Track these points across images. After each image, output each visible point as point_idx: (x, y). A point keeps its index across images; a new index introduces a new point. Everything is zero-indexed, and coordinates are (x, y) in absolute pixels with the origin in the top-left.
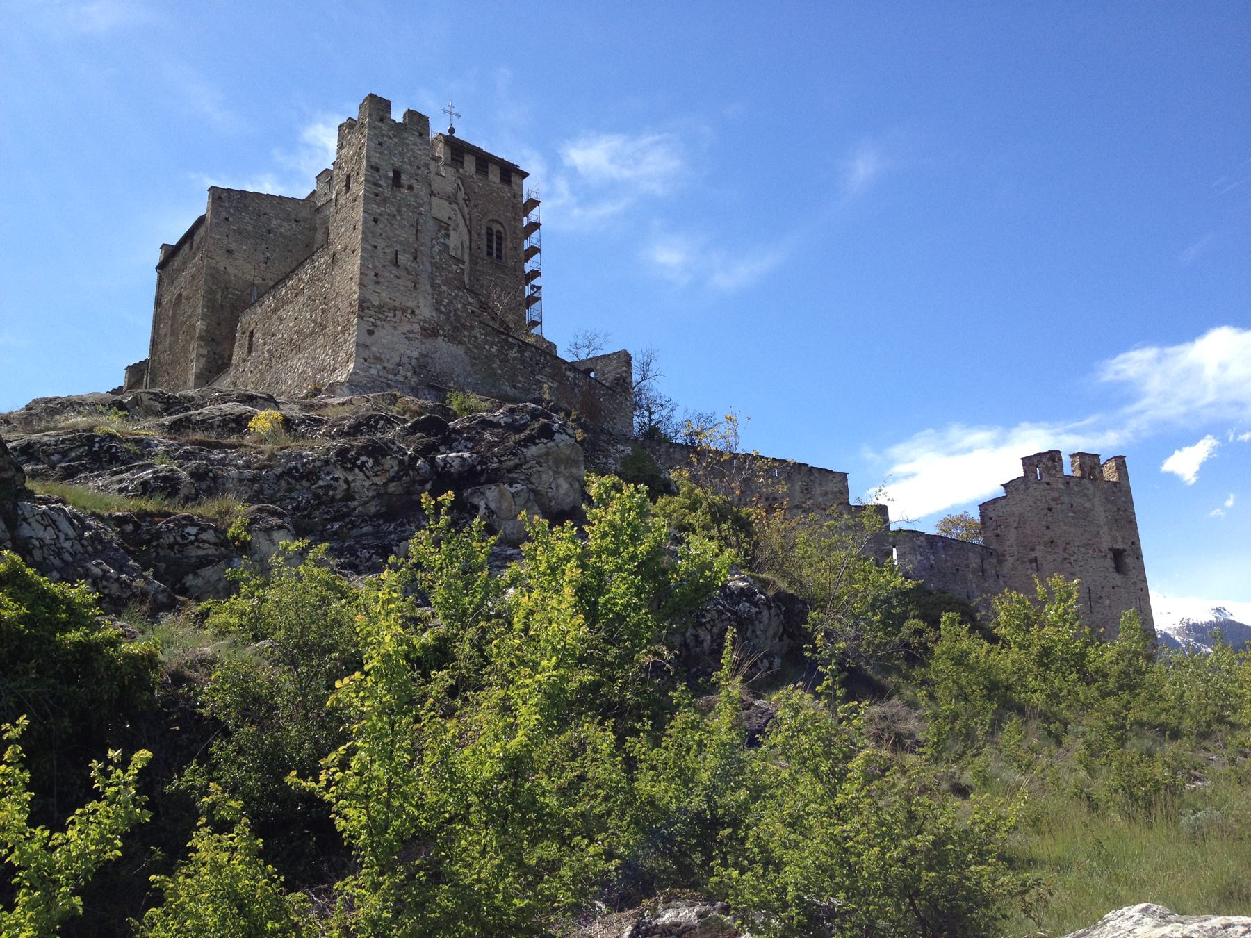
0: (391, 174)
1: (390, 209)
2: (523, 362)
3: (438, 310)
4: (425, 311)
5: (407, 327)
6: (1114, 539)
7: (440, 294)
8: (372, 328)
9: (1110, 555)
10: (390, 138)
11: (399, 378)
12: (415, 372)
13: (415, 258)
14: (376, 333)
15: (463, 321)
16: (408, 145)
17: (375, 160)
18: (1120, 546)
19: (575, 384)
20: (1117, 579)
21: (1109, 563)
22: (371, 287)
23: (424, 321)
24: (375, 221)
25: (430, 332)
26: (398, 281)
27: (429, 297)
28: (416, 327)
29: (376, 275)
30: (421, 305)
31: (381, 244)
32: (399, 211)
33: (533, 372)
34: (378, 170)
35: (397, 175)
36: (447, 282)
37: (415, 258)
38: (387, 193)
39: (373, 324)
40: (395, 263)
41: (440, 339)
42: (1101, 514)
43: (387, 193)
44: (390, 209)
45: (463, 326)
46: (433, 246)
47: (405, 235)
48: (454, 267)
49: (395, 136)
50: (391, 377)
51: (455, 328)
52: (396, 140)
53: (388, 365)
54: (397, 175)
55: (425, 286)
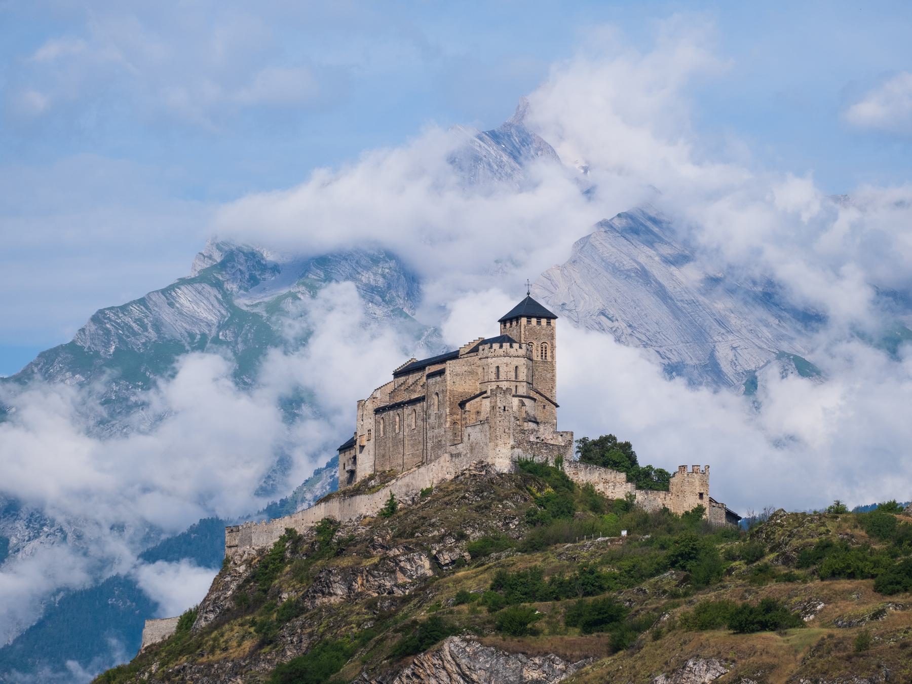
1: (503, 418)
2: (537, 448)
6: (701, 490)
18: (702, 492)
21: (698, 497)
35: (504, 407)
38: (502, 414)
42: (697, 483)
43: (502, 414)
44: (503, 418)
51: (519, 445)
54: (504, 407)
55: (512, 436)
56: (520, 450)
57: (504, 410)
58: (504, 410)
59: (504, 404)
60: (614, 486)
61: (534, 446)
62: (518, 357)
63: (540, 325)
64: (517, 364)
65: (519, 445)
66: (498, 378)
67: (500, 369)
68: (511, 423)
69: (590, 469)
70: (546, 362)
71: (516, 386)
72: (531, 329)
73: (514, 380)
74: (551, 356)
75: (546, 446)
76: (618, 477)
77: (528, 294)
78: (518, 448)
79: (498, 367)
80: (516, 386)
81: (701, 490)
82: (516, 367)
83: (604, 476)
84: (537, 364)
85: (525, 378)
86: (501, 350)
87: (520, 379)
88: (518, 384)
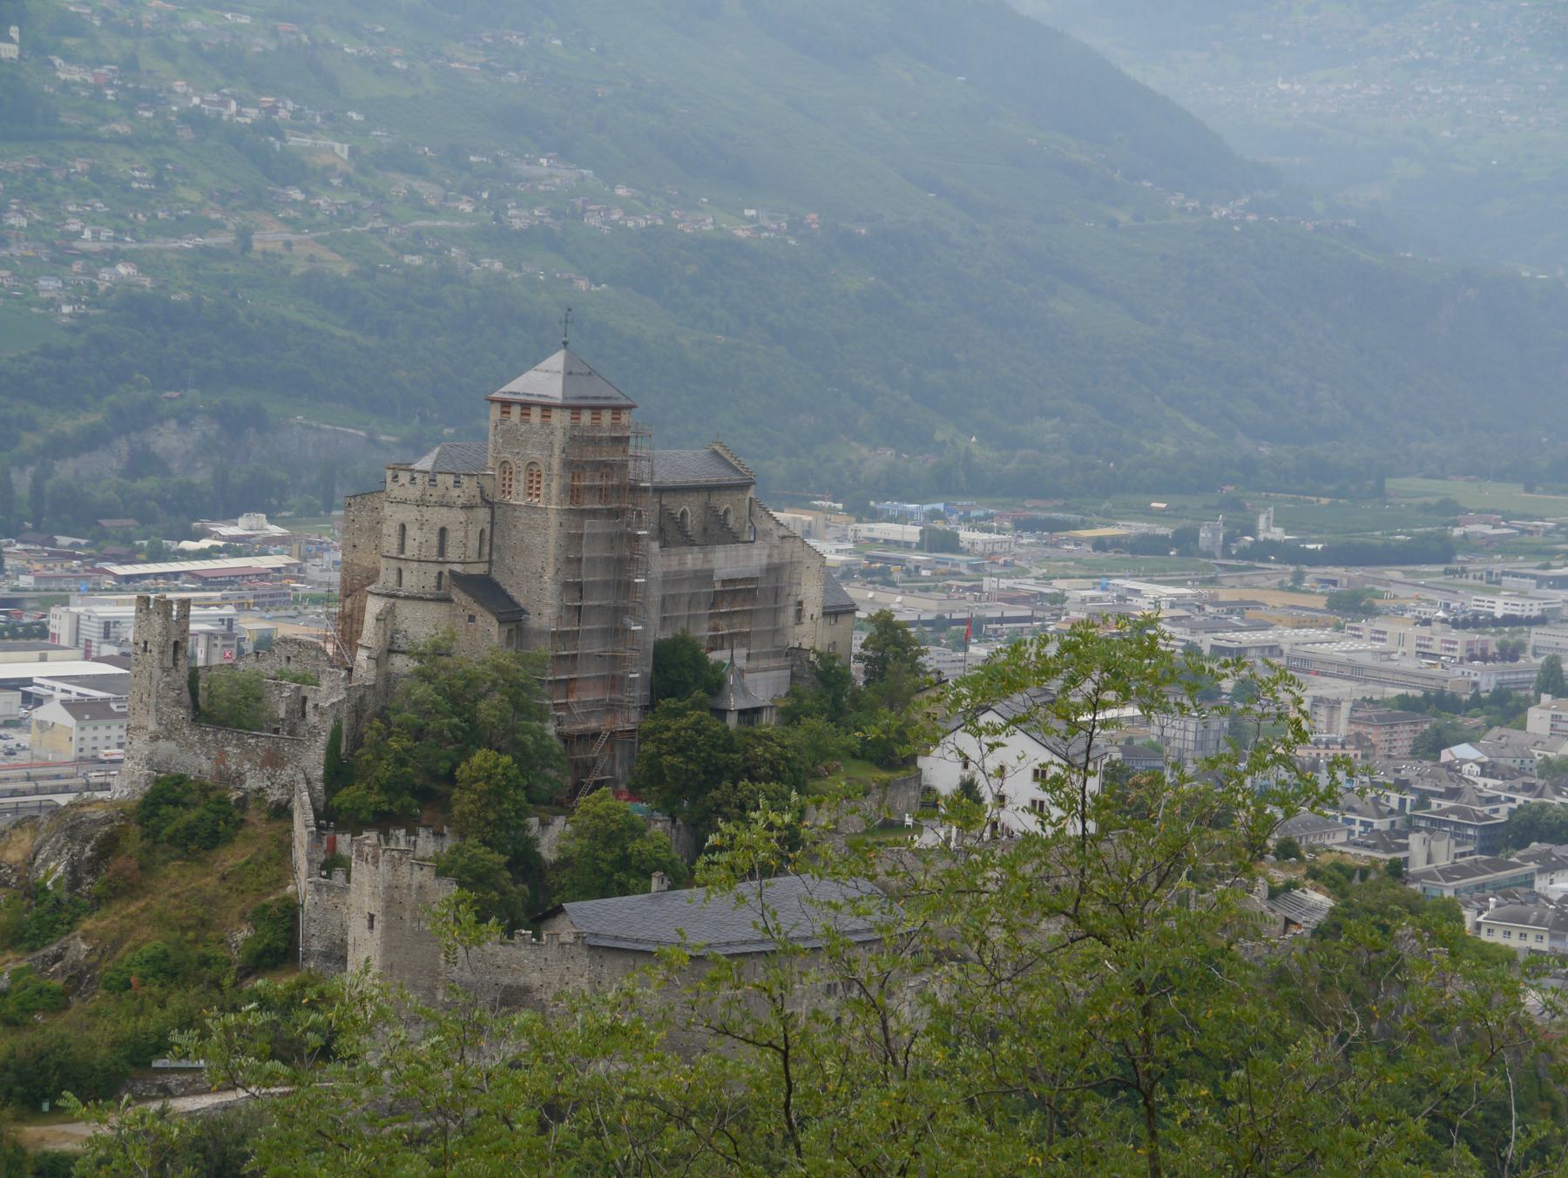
2: (216, 741)
3: (160, 724)
7: (163, 714)
25: (155, 738)
35: (146, 643)
43: (140, 657)
47: (146, 682)
54: (146, 643)
55: (153, 712)
56: (172, 745)
57: (145, 649)
58: (145, 649)
59: (145, 636)
61: (210, 737)
62: (405, 502)
63: (527, 422)
68: (154, 683)
71: (400, 571)
72: (508, 431)
75: (238, 740)
78: (168, 738)
80: (400, 571)
82: (403, 527)
84: (517, 514)
87: (408, 554)
88: (402, 565)
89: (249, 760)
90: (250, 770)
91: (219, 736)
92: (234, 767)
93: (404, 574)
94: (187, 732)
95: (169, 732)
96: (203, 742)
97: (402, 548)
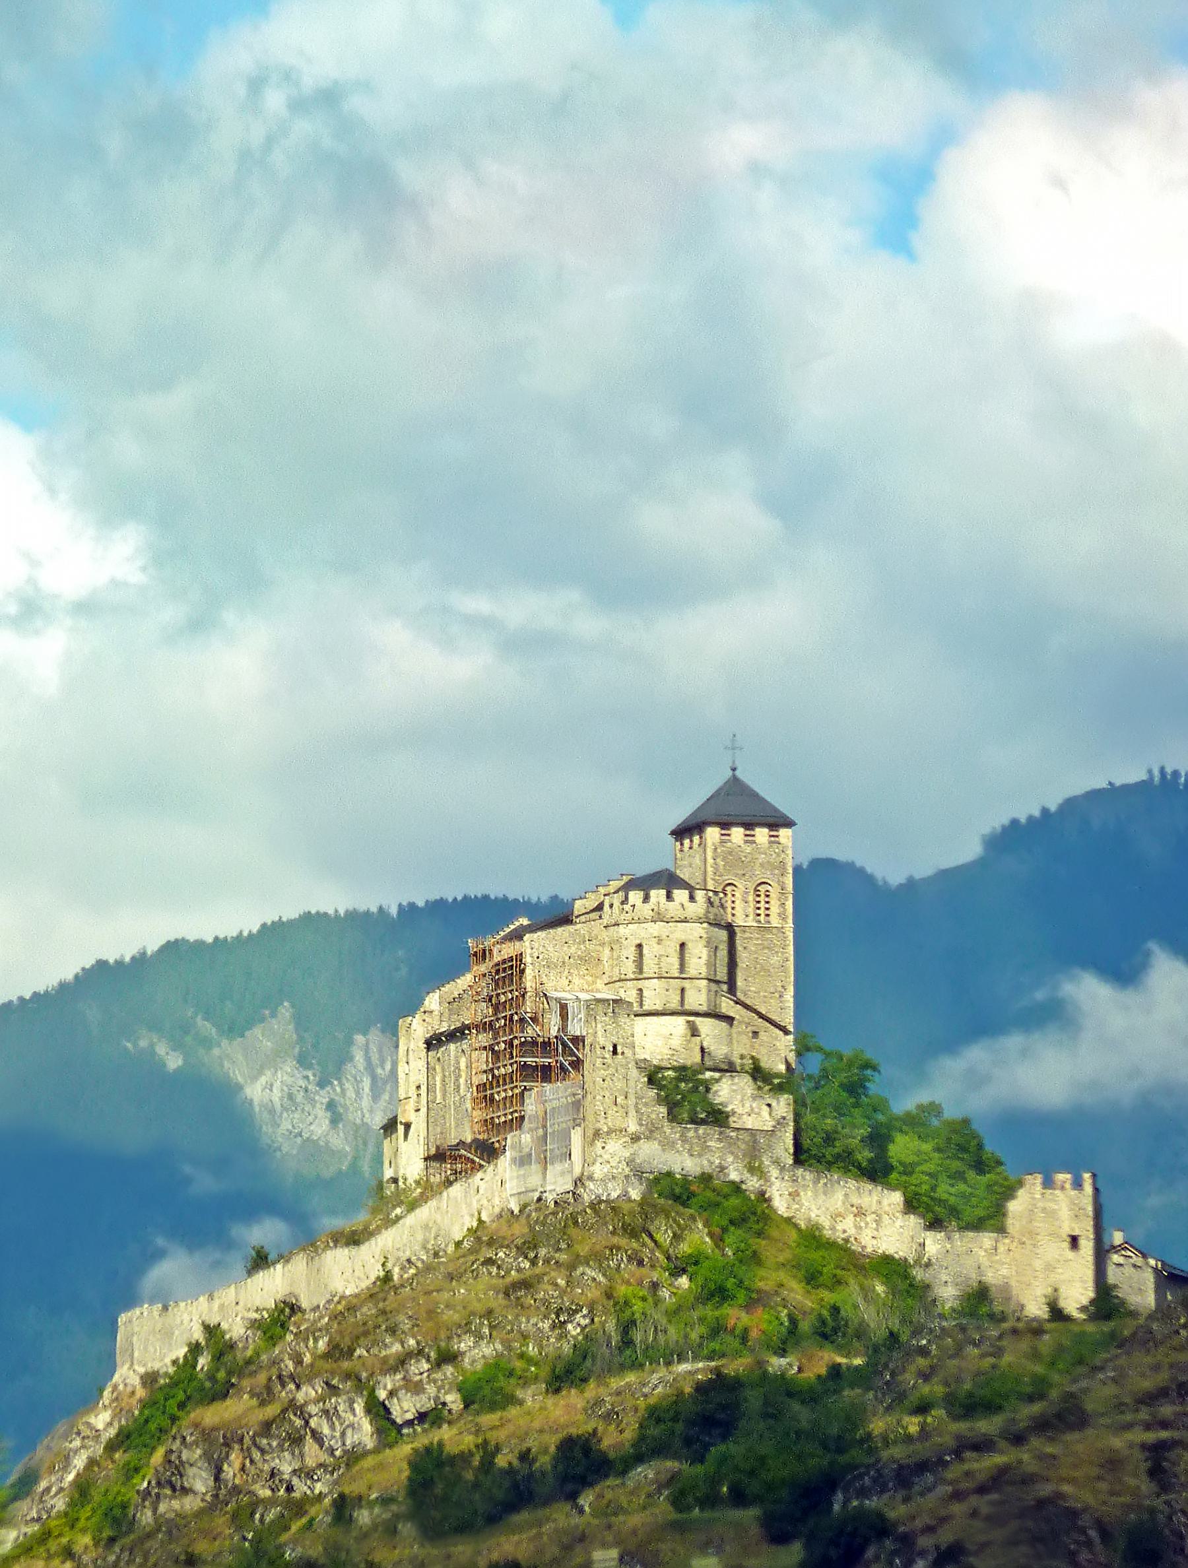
0: (611, 1049)
2: (698, 1137)
3: (641, 1125)
4: (633, 1127)
5: (624, 1140)
8: (604, 1145)
9: (1069, 1239)
10: (610, 1025)
11: (620, 1170)
12: (628, 1165)
13: (626, 1098)
14: (606, 1148)
15: (656, 1126)
16: (621, 1025)
17: (602, 1043)
19: (738, 1139)
20: (1070, 1254)
21: (1066, 1245)
22: (603, 1121)
23: (633, 1134)
24: (604, 1080)
25: (635, 1139)
26: (618, 1114)
27: (634, 1119)
28: (627, 1139)
29: (605, 1113)
30: (630, 1125)
31: (607, 1095)
32: (617, 1071)
33: (705, 1142)
34: (604, 1048)
35: (615, 1047)
36: (646, 1104)
37: (626, 1098)
38: (609, 1061)
39: (605, 1142)
40: (616, 1104)
41: (642, 1141)
43: (609, 1061)
45: (657, 1128)
46: (636, 1086)
47: (619, 1085)
48: (650, 1094)
49: (613, 1023)
50: (615, 1171)
51: (651, 1132)
52: (614, 1025)
53: (614, 1165)
54: (615, 1047)
55: (632, 1113)
57: (615, 1052)
58: (615, 1052)
60: (878, 1222)
62: (685, 921)
64: (682, 937)
65: (651, 1132)
66: (682, 966)
67: (645, 951)
68: (632, 1083)
69: (825, 1184)
70: (768, 929)
71: (683, 990)
72: (730, 853)
73: (677, 975)
74: (779, 914)
76: (885, 1202)
77: (734, 770)
79: (640, 946)
80: (683, 990)
81: (1073, 1229)
82: (682, 945)
83: (855, 1200)
85: (704, 971)
86: (648, 906)
88: (686, 984)
89: (732, 1153)
90: (733, 1163)
91: (701, 1131)
92: (717, 1161)
93: (687, 994)
94: (668, 1131)
95: (651, 1131)
96: (684, 1140)
97: (682, 966)
